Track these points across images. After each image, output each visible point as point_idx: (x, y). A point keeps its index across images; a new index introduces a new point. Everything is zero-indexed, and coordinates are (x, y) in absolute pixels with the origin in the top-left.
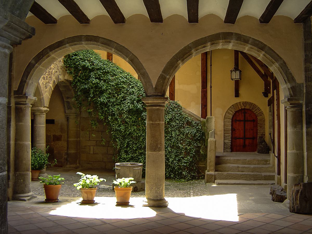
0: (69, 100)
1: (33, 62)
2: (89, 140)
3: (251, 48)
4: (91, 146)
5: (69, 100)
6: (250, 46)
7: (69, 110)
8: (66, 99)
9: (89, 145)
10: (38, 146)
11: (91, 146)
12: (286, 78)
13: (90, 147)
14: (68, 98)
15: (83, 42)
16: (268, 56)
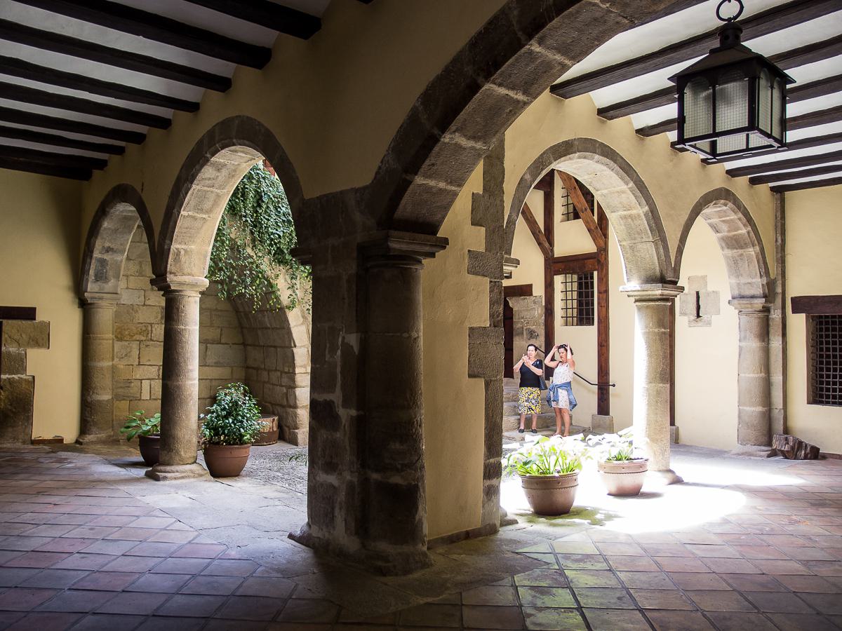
0: (107, 257)
1: (528, 177)
2: (139, 365)
3: (740, 219)
4: (143, 381)
5: (107, 257)
6: (740, 215)
7: (99, 283)
8: (100, 253)
9: (138, 377)
10: (192, 384)
11: (143, 381)
12: (764, 270)
13: (141, 383)
14: (108, 250)
15: (597, 157)
16: (752, 234)
